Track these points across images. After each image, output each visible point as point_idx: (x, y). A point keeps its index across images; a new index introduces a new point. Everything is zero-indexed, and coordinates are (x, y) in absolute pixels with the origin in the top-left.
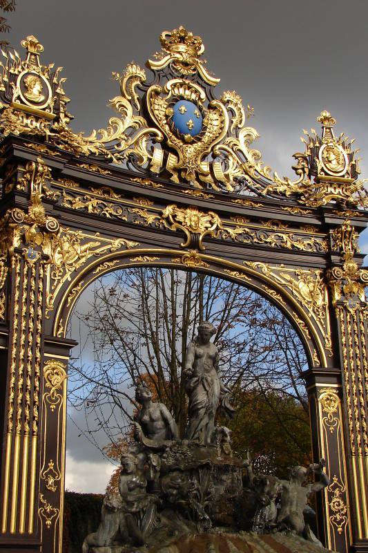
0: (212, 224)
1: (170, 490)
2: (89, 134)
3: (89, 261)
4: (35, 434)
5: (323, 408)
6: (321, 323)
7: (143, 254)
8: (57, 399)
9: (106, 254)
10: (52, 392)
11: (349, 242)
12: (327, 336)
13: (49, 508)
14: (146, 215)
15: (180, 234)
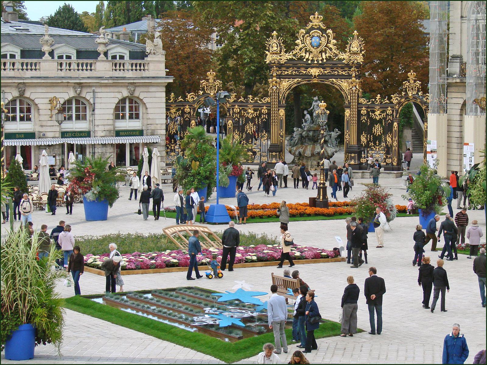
2: (290, 53)
15: (311, 75)
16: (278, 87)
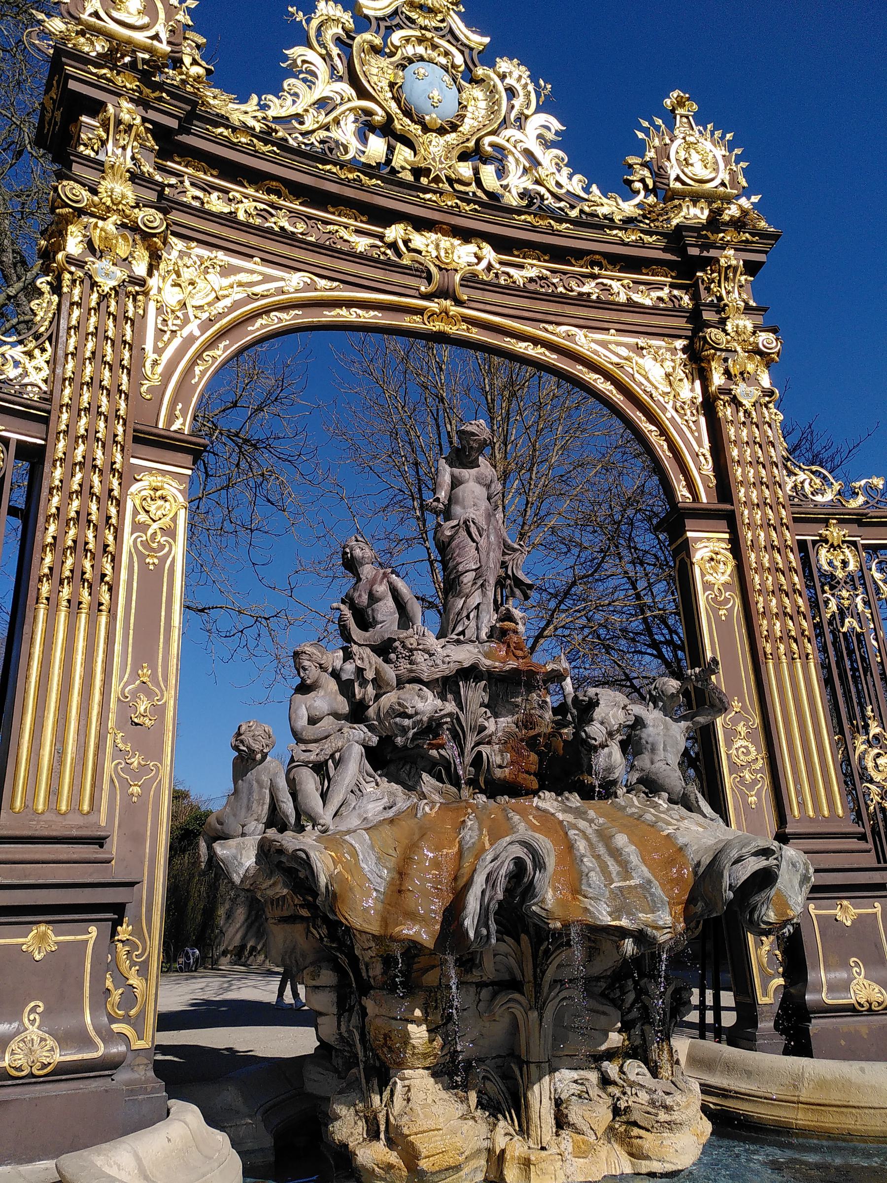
0: (479, 259)
1: (398, 719)
3: (236, 305)
4: (103, 608)
5: (703, 575)
6: (689, 427)
7: (350, 304)
8: (162, 547)
9: (272, 295)
10: (150, 532)
11: (733, 288)
12: (702, 450)
13: (135, 762)
14: (353, 238)
16: (140, 268)
